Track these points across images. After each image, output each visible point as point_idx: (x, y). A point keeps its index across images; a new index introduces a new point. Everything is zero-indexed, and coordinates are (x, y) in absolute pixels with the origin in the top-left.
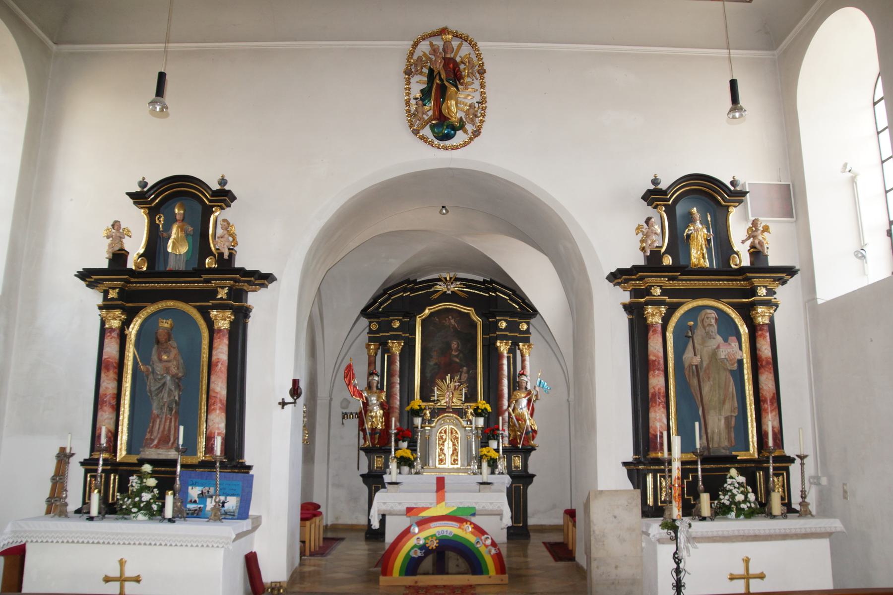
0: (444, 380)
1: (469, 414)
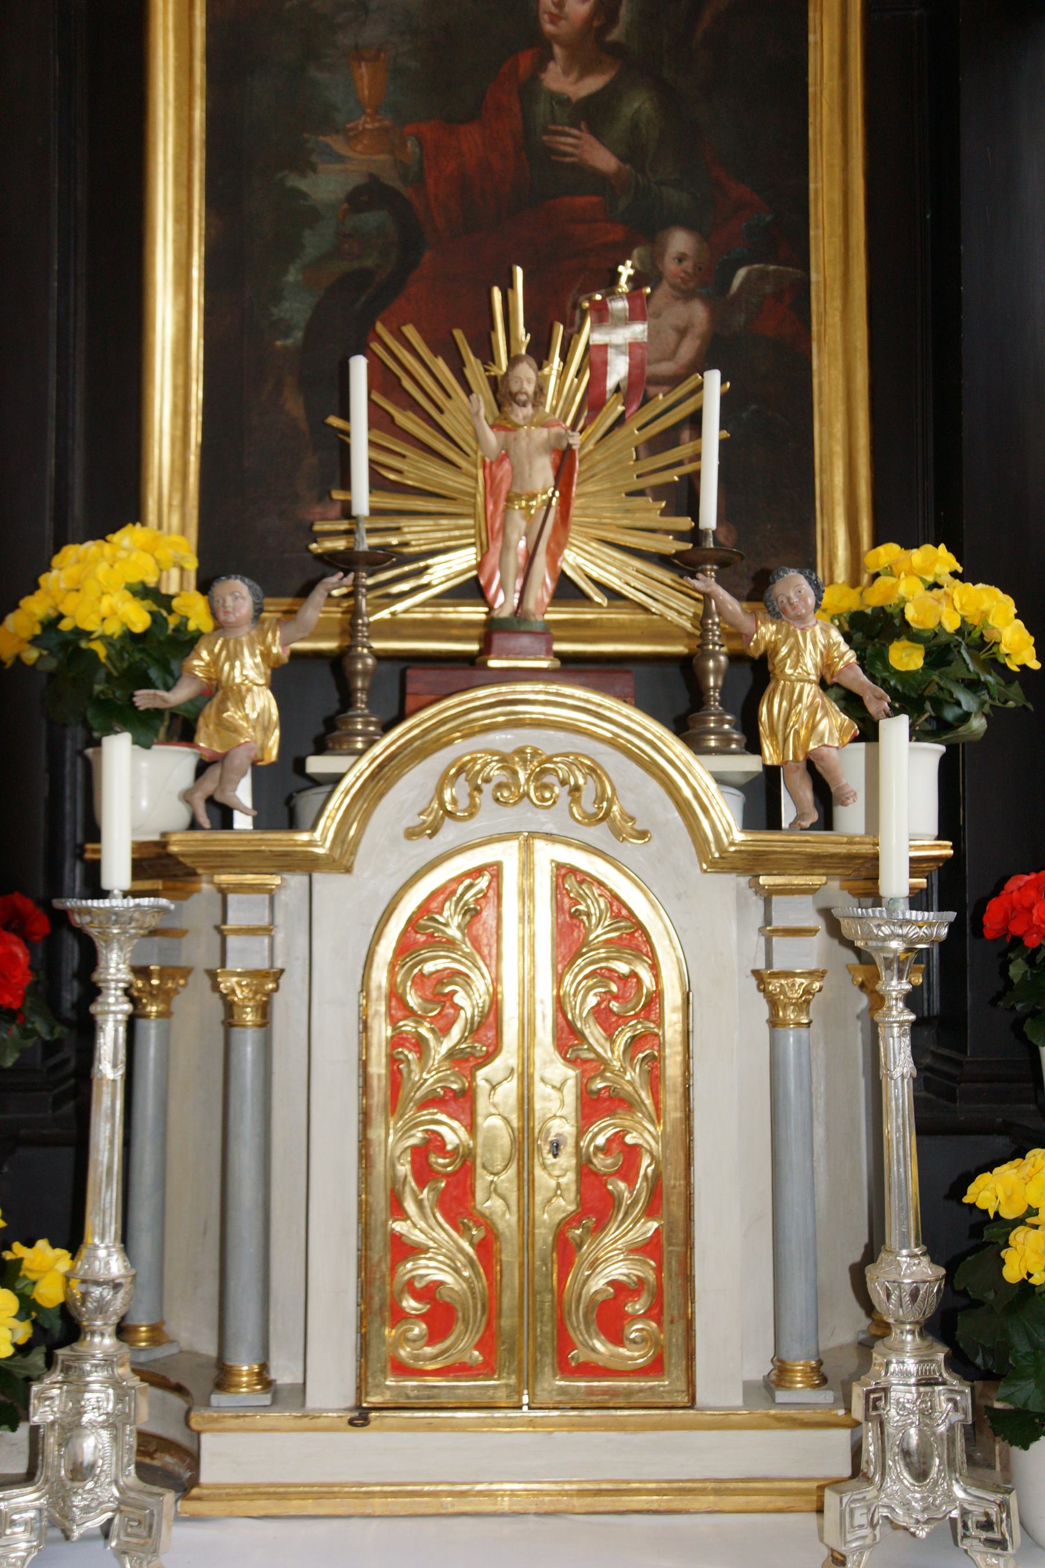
0: (458, 334)
1: (810, 691)
